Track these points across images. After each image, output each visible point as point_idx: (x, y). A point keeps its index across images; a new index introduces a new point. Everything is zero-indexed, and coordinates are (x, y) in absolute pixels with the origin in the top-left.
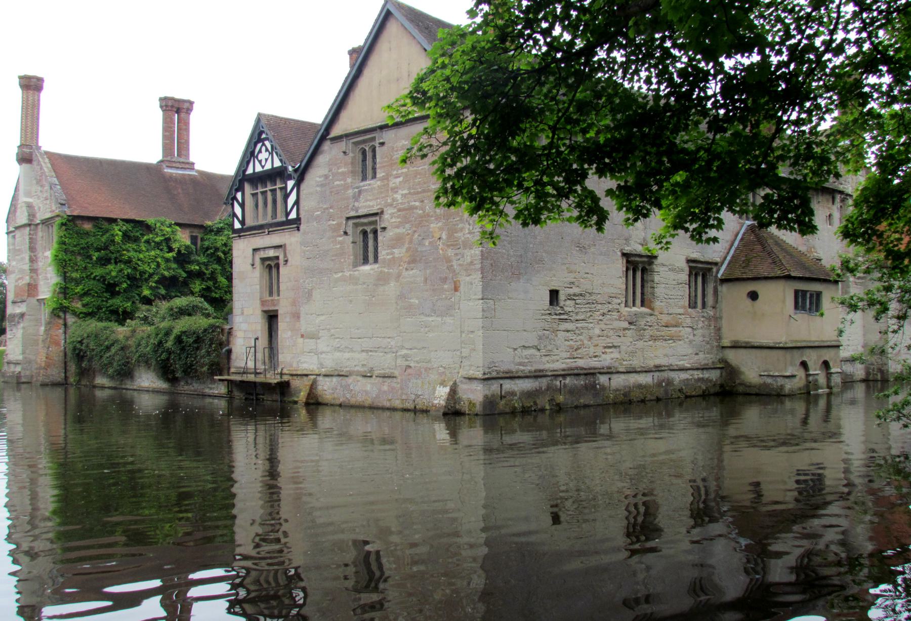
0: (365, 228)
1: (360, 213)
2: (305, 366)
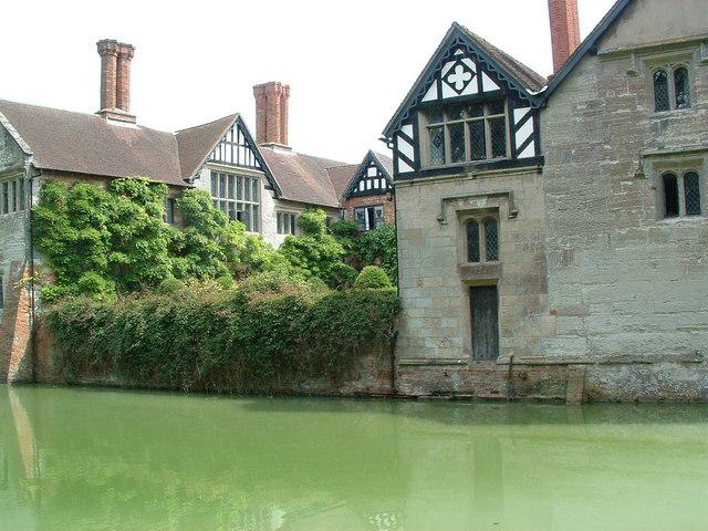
0: (673, 169)
1: (670, 148)
2: (561, 352)
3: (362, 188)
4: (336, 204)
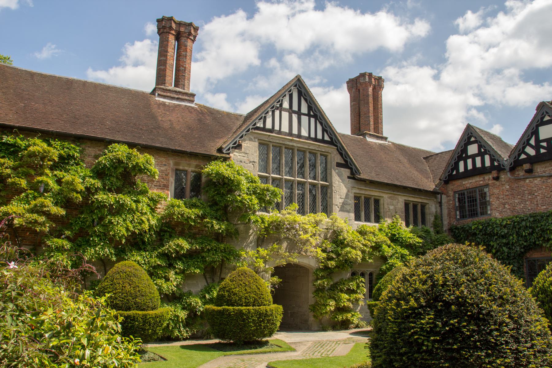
3: (462, 169)
4: (431, 186)
